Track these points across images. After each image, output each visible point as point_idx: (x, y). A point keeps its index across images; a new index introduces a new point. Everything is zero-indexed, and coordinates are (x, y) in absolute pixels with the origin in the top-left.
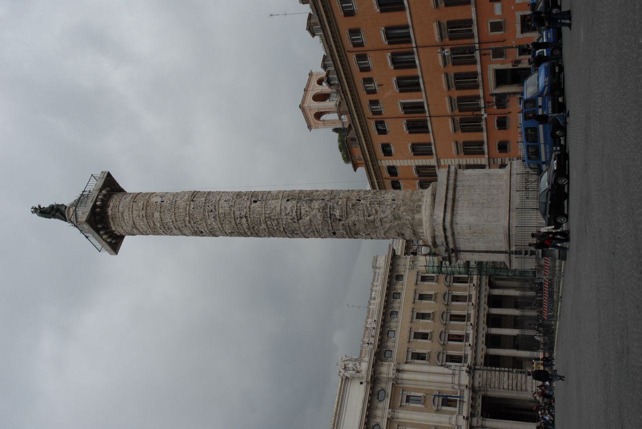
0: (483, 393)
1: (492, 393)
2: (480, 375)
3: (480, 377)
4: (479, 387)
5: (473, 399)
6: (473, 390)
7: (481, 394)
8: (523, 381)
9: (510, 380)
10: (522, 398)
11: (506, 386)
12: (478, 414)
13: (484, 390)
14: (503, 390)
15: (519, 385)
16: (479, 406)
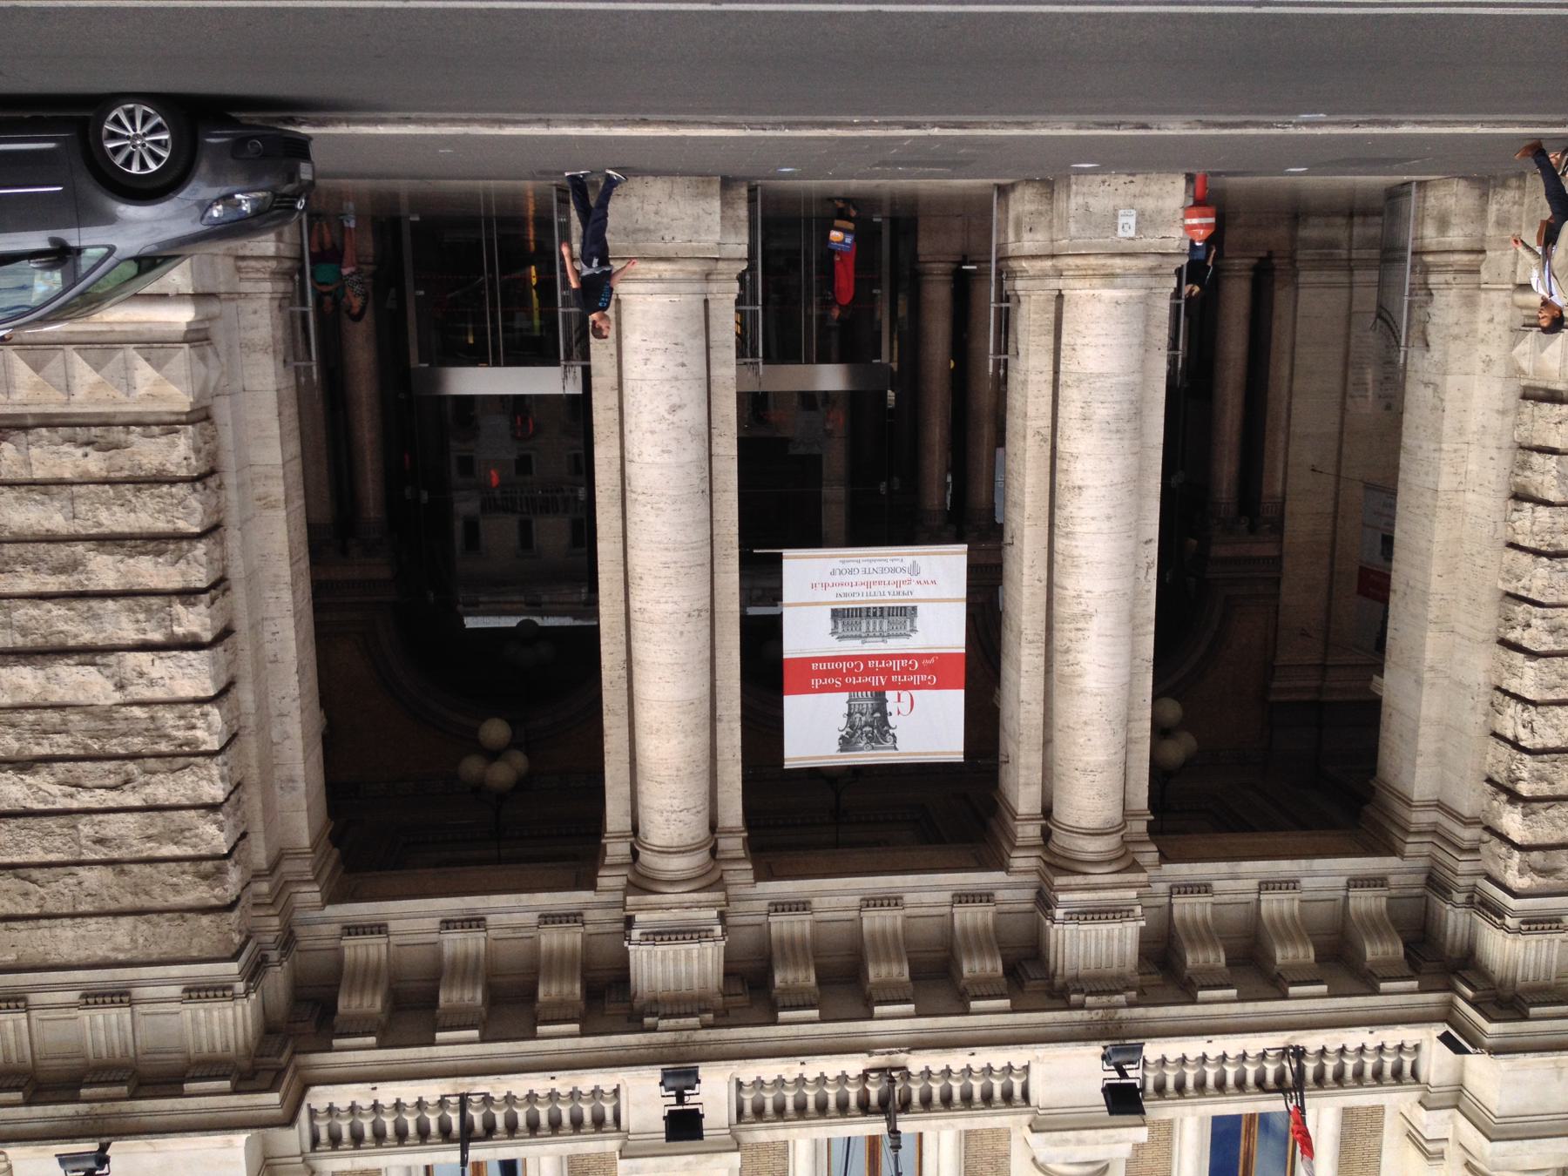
0: (310, 894)
1: (299, 813)
2: (94, 997)
3: (120, 996)
4: (255, 972)
5: (412, 1009)
6: (305, 1020)
7: (325, 920)
8: (69, 460)
9: (86, 635)
10: (294, 447)
11: (189, 676)
12: (573, 917)
13: (280, 899)
14: (245, 694)
15: (144, 515)
16: (475, 922)
